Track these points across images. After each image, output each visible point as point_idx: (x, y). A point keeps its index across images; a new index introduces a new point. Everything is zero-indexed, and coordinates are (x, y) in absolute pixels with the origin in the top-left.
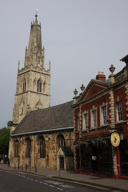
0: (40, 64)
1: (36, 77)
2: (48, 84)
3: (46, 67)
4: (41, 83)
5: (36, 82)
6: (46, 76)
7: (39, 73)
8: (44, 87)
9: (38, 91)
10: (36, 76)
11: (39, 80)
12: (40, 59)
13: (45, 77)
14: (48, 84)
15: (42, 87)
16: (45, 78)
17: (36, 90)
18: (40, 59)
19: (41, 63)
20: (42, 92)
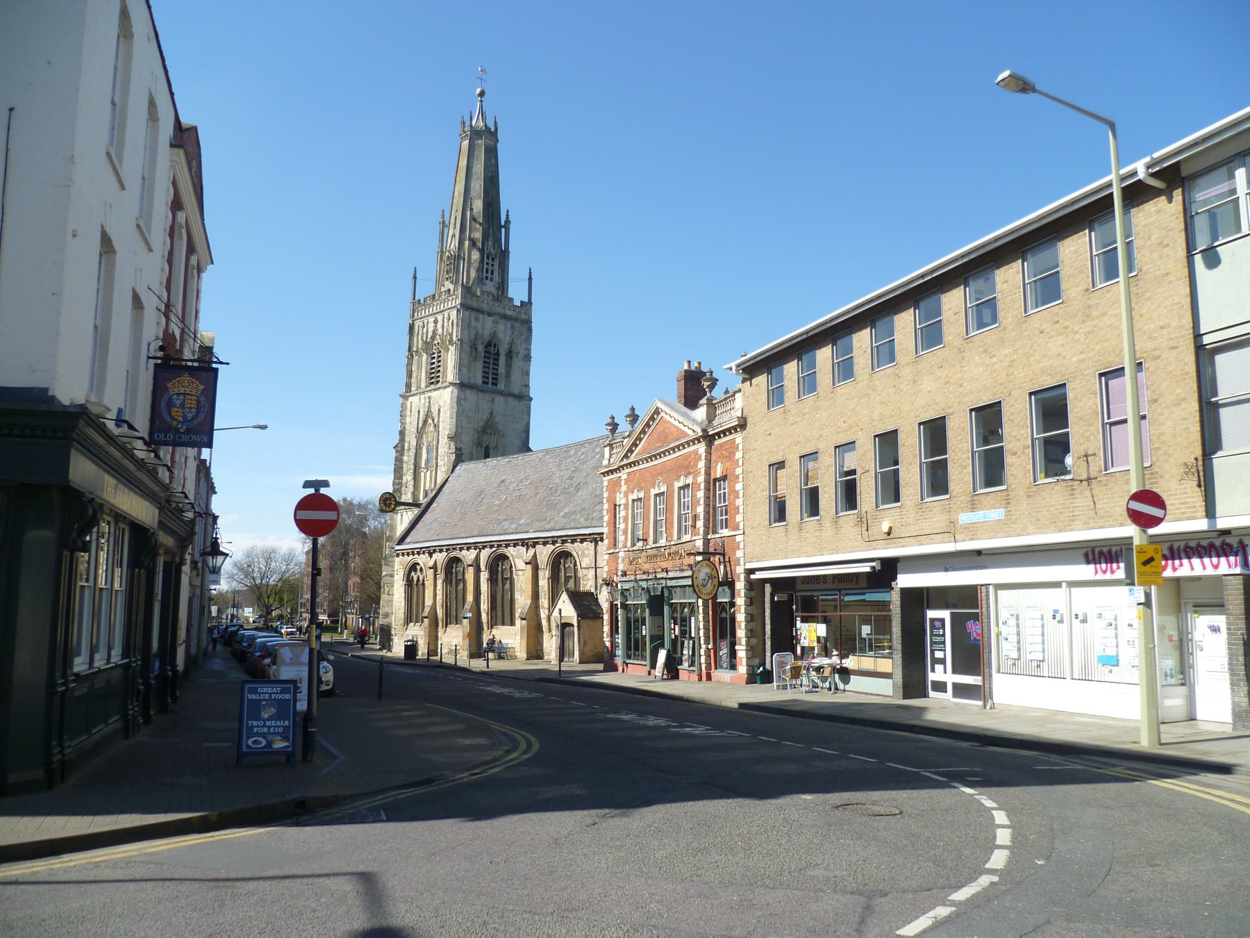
0: (492, 279)
1: (480, 332)
2: (521, 356)
3: (517, 292)
4: (498, 354)
5: (481, 348)
6: (517, 325)
7: (490, 315)
8: (509, 366)
9: (487, 383)
10: (479, 325)
11: (489, 344)
12: (493, 259)
13: (512, 327)
14: (521, 356)
15: (502, 369)
16: (513, 333)
17: (479, 381)
18: (493, 259)
19: (496, 276)
20: (501, 386)
